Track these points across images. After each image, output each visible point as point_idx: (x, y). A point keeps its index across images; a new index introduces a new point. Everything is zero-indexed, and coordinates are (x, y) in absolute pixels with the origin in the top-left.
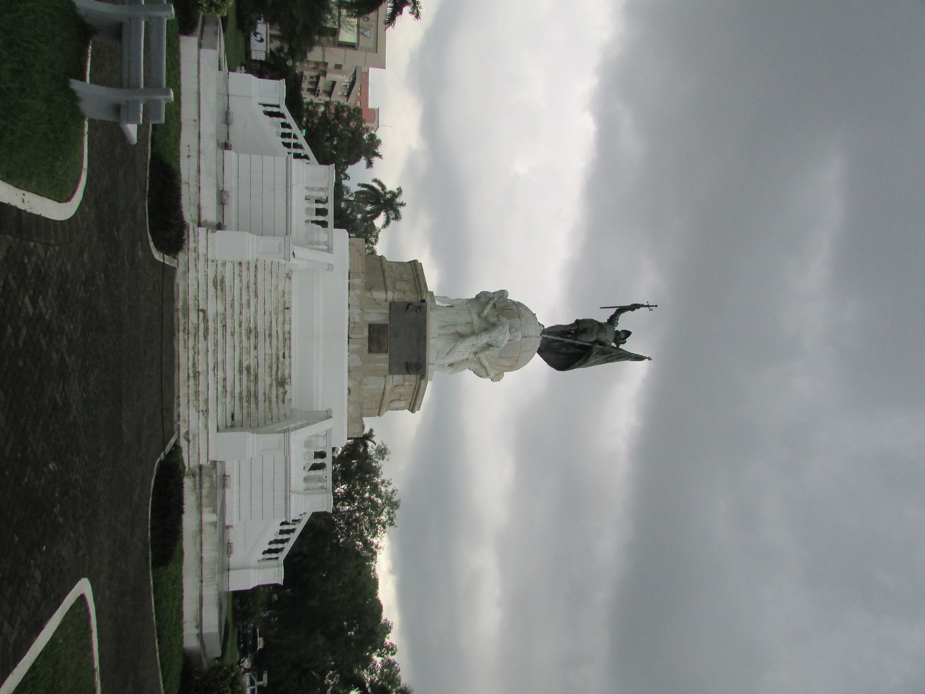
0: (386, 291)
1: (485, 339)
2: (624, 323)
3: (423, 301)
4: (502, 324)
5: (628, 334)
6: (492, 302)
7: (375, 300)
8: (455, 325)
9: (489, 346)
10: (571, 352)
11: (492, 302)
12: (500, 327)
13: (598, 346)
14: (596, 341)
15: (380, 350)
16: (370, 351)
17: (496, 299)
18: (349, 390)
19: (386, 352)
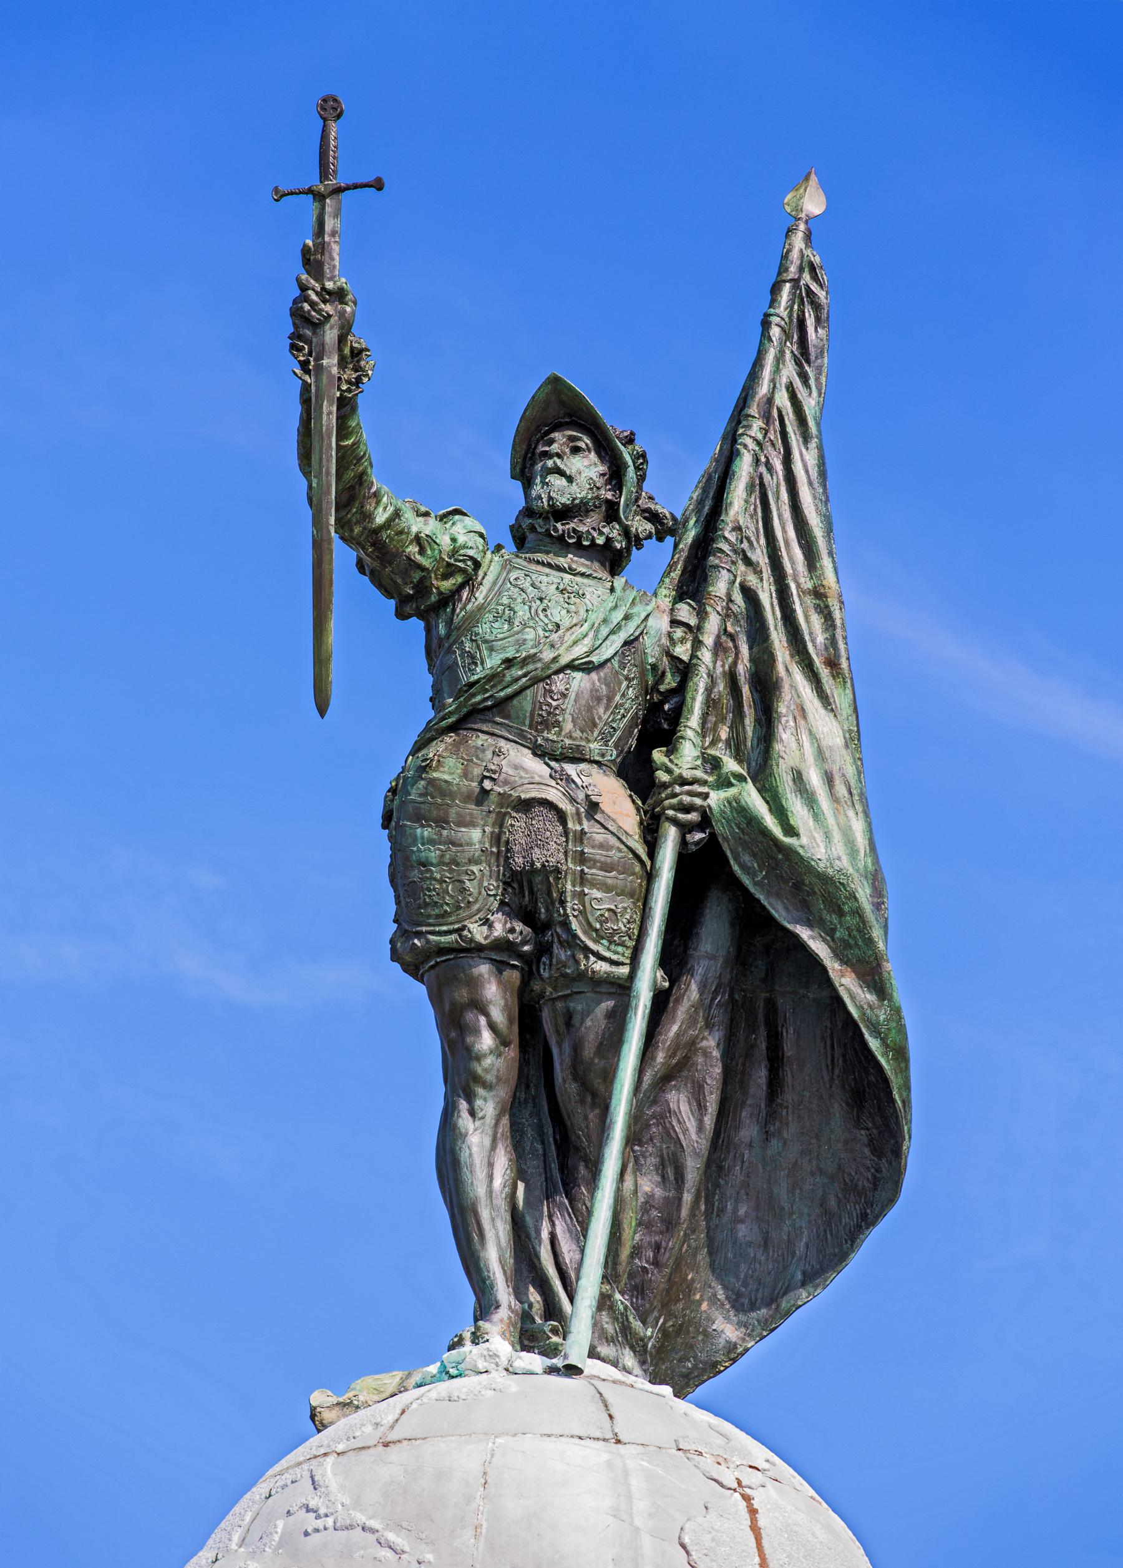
10: (711, 1043)
13: (687, 757)
14: (637, 774)
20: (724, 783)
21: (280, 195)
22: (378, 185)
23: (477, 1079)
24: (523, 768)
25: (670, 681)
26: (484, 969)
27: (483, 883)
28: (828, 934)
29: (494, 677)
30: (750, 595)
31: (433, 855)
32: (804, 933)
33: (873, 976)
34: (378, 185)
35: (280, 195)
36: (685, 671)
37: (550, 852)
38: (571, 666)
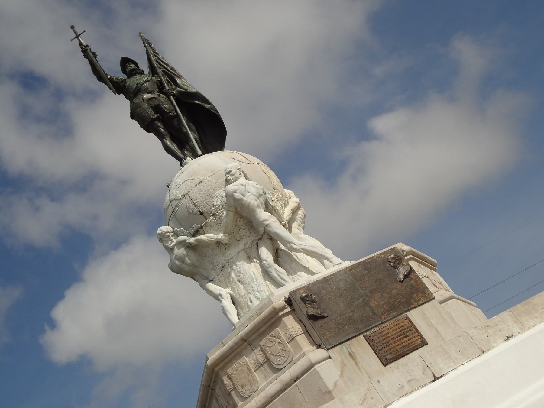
0: (311, 366)
1: (263, 215)
2: (113, 69)
3: (289, 302)
4: (229, 196)
5: (125, 62)
6: (192, 240)
7: (342, 375)
8: (266, 273)
9: (269, 208)
11: (192, 240)
12: (237, 195)
15: (411, 329)
16: (424, 343)
17: (182, 238)
18: (508, 338)
19: (407, 318)
20: (174, 89)
21: (72, 40)
22: (84, 31)
23: (164, 135)
24: (147, 96)
25: (159, 84)
26: (156, 122)
27: (150, 111)
28: (199, 100)
29: (136, 87)
30: (163, 71)
31: (141, 111)
32: (196, 102)
33: (208, 102)
34: (84, 31)
35: (72, 40)
36: (161, 81)
37: (157, 102)
38: (146, 81)
